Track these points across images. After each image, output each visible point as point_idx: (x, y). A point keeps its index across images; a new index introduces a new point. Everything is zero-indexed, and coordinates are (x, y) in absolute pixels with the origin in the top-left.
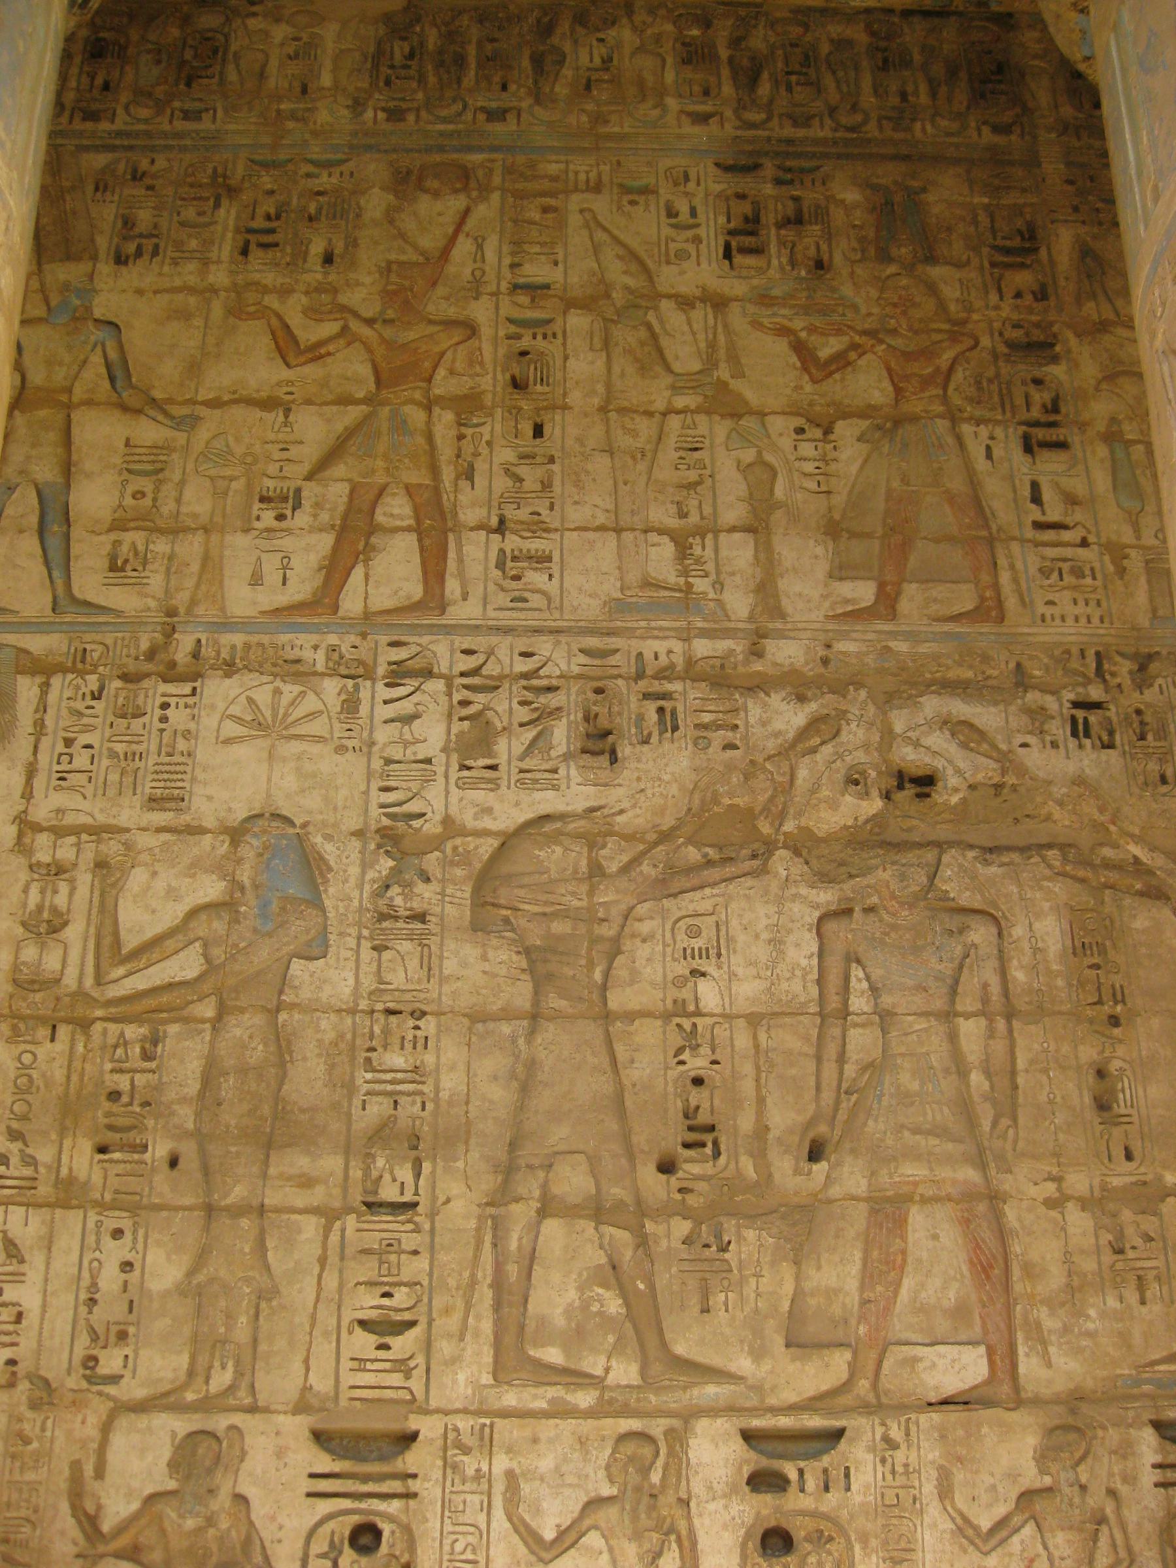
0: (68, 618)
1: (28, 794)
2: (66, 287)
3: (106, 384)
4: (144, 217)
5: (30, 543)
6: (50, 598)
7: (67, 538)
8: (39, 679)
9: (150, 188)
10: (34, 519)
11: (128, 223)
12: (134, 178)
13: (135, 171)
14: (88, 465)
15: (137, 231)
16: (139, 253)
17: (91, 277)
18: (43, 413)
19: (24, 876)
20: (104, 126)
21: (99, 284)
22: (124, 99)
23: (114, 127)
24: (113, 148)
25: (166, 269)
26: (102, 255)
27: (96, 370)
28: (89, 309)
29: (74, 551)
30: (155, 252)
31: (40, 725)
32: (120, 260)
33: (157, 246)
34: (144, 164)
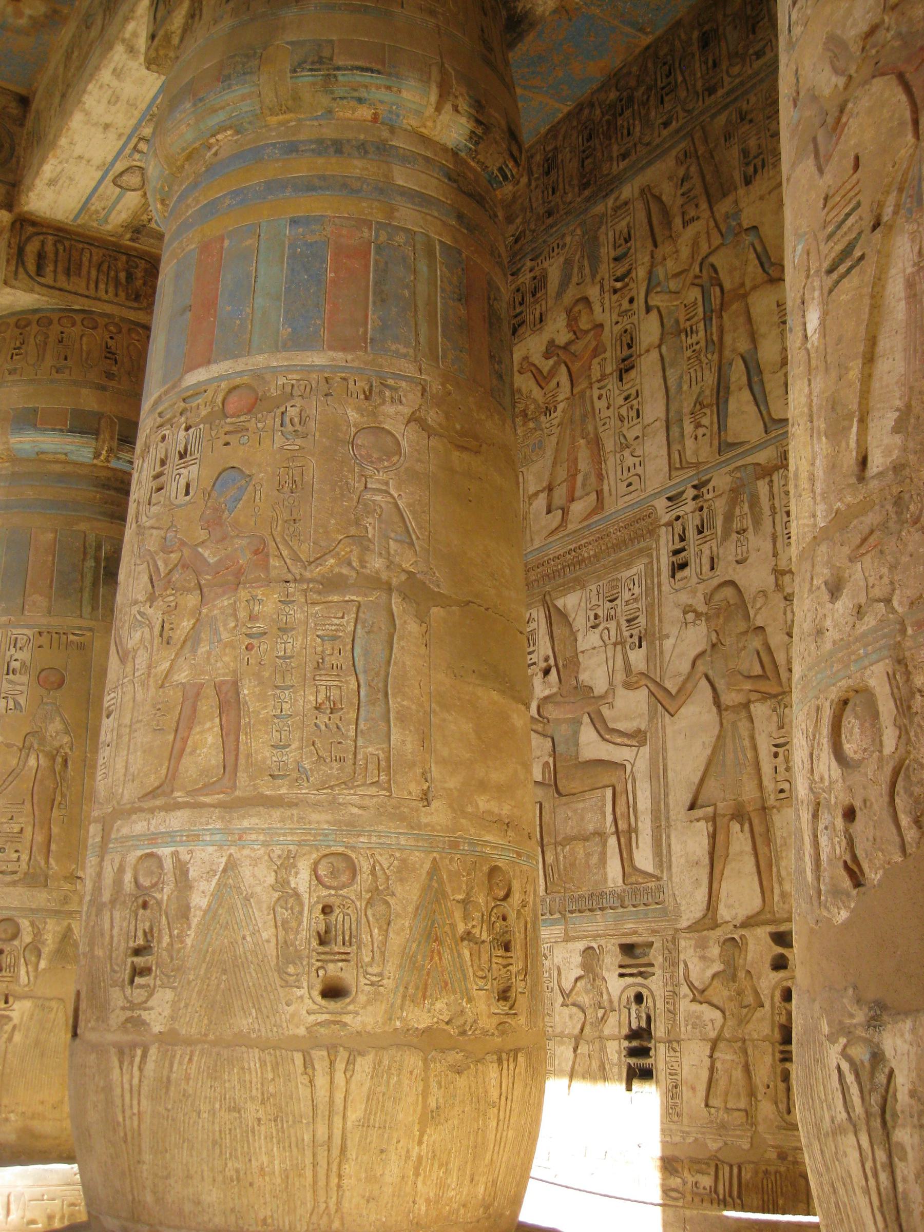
0: (773, 434)
1: (775, 555)
2: (727, 216)
3: (760, 270)
4: (752, 143)
5: (746, 395)
6: (762, 425)
7: (762, 382)
8: (767, 479)
9: (751, 121)
10: (745, 378)
11: (745, 153)
12: (742, 119)
13: (741, 114)
14: (763, 329)
15: (751, 156)
16: (755, 172)
17: (736, 202)
18: (734, 307)
19: (783, 604)
20: (720, 92)
21: (742, 205)
22: (724, 68)
23: (725, 90)
24: (726, 106)
25: (771, 173)
26: (738, 184)
27: (753, 266)
28: (740, 225)
29: (767, 390)
30: (763, 167)
31: (773, 508)
32: (748, 182)
33: (763, 160)
34: (745, 107)
